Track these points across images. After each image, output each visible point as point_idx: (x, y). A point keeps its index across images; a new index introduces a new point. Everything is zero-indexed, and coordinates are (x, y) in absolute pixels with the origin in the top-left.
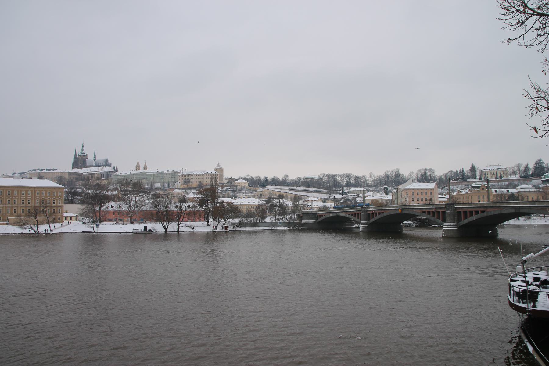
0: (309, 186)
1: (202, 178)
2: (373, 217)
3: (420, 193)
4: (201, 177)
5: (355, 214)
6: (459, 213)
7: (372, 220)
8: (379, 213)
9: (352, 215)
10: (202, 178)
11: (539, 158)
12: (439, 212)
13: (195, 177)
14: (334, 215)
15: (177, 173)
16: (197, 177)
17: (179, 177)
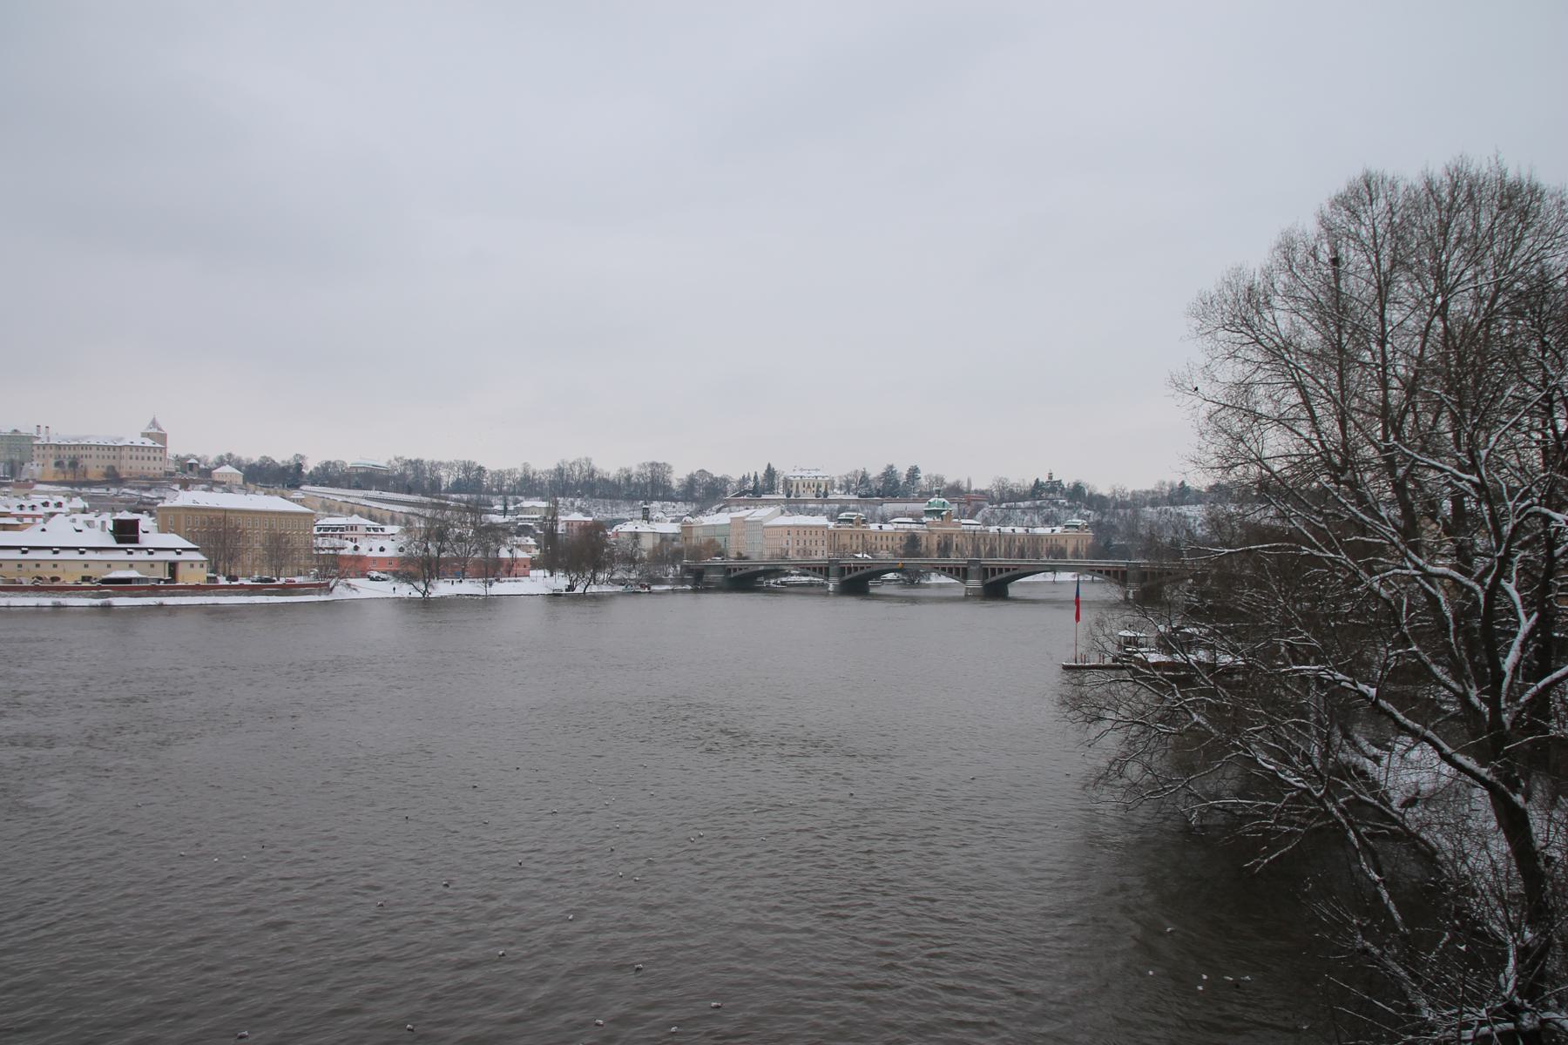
0: (409, 492)
1: (114, 457)
2: (850, 572)
3: (802, 533)
4: (112, 453)
5: (821, 569)
6: (986, 570)
7: (847, 577)
8: (862, 568)
9: (809, 569)
10: (114, 457)
11: (890, 464)
12: (958, 569)
13: (94, 452)
14: (769, 568)
15: (30, 438)
16: (101, 453)
17: (35, 448)
